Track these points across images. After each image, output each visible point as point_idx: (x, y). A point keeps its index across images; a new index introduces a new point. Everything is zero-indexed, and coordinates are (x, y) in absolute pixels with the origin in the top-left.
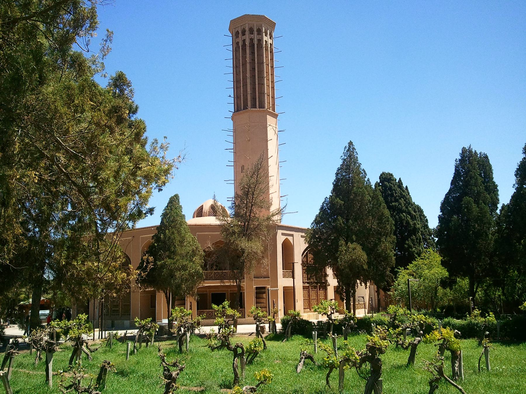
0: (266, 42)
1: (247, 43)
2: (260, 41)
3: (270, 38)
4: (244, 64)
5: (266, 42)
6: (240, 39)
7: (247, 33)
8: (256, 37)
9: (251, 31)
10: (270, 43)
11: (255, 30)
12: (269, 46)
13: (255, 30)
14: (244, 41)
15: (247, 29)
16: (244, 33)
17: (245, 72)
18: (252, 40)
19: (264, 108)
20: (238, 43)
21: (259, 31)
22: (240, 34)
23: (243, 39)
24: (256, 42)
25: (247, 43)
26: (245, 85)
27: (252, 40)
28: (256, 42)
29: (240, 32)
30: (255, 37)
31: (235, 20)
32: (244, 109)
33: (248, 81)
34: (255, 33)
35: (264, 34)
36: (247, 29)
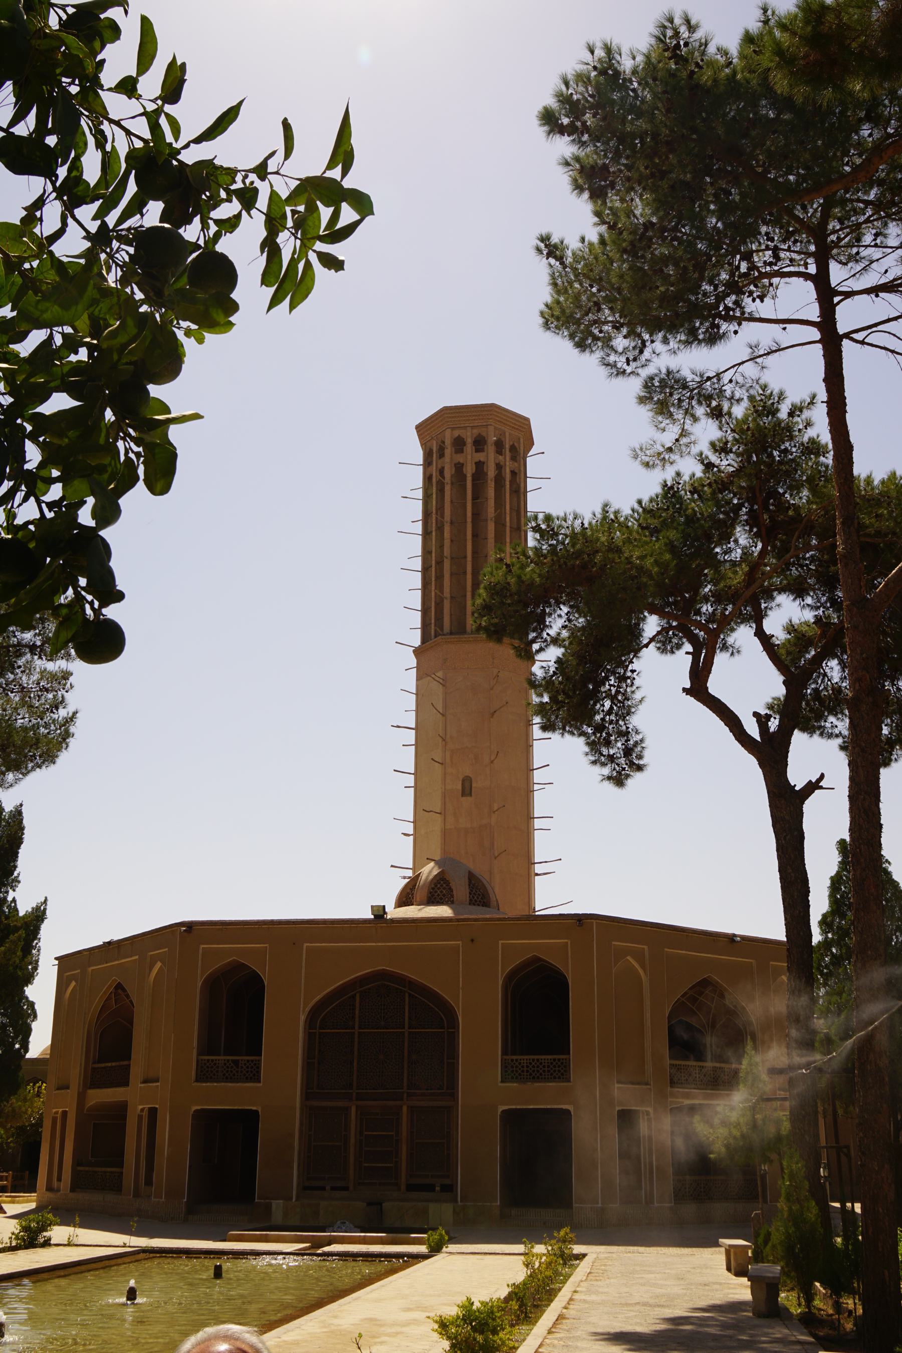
1: (448, 474)
2: (480, 465)
3: (514, 458)
4: (440, 529)
5: (499, 467)
6: (434, 468)
7: (448, 452)
8: (469, 458)
9: (459, 444)
10: (514, 473)
11: (469, 441)
12: (508, 476)
14: (441, 472)
15: (448, 442)
16: (441, 455)
17: (441, 547)
18: (459, 468)
20: (428, 479)
21: (479, 444)
22: (434, 455)
23: (439, 466)
24: (469, 470)
25: (448, 474)
26: (440, 577)
27: (459, 468)
28: (469, 470)
29: (435, 449)
30: (469, 457)
32: (436, 637)
33: (447, 565)
34: (469, 448)
35: (491, 449)
36: (448, 442)
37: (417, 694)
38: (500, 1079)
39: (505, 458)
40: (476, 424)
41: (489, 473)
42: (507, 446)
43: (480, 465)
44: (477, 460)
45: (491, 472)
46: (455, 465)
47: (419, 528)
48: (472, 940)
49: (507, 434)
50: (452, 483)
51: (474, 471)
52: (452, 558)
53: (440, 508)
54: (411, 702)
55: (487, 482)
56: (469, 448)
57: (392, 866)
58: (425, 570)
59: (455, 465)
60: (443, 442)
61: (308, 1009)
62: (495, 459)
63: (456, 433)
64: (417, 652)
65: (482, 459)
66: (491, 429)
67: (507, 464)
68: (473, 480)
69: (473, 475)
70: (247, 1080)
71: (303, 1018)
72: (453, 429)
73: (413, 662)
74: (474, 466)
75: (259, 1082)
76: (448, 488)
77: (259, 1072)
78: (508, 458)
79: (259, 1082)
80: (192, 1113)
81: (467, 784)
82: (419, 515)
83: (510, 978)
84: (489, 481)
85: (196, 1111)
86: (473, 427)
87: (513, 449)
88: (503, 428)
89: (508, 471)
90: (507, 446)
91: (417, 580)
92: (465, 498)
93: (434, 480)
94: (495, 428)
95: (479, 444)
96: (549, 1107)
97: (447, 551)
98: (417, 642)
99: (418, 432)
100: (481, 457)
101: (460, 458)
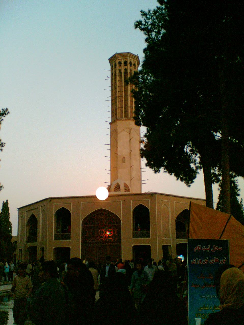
0: (131, 70)
2: (126, 70)
5: (131, 70)
9: (120, 63)
11: (123, 63)
13: (123, 63)
14: (115, 72)
16: (116, 67)
18: (120, 71)
19: (128, 117)
20: (112, 74)
21: (125, 63)
22: (113, 67)
26: (116, 102)
27: (120, 71)
28: (123, 71)
29: (113, 65)
31: (110, 58)
33: (118, 99)
34: (123, 65)
35: (129, 65)
37: (110, 135)
38: (132, 238)
39: (132, 68)
40: (124, 58)
41: (128, 72)
42: (133, 64)
43: (126, 70)
44: (124, 68)
45: (129, 71)
46: (119, 70)
47: (110, 88)
48: (124, 200)
49: (133, 61)
50: (118, 75)
51: (124, 72)
52: (119, 97)
53: (116, 82)
54: (109, 137)
55: (127, 74)
56: (123, 65)
57: (105, 182)
58: (112, 100)
59: (119, 70)
60: (116, 63)
61: (82, 220)
62: (130, 68)
63: (119, 61)
64: (110, 124)
65: (126, 68)
66: (128, 59)
67: (133, 69)
68: (124, 74)
69: (124, 73)
70: (67, 239)
71: (81, 223)
72: (118, 60)
73: (109, 126)
74: (124, 70)
75: (70, 240)
76: (117, 77)
77: (70, 237)
78: (133, 68)
79: (70, 240)
80: (53, 248)
81: (124, 160)
82: (110, 85)
83: (134, 210)
84: (128, 74)
85: (54, 248)
86: (124, 59)
87: (134, 65)
88: (132, 59)
89: (133, 71)
90: (133, 64)
91: (109, 103)
92: (122, 80)
93: (114, 74)
94: (130, 59)
95: (125, 63)
96: (145, 244)
97: (117, 95)
98: (110, 121)
99: (109, 60)
100: (126, 67)
101: (120, 68)
